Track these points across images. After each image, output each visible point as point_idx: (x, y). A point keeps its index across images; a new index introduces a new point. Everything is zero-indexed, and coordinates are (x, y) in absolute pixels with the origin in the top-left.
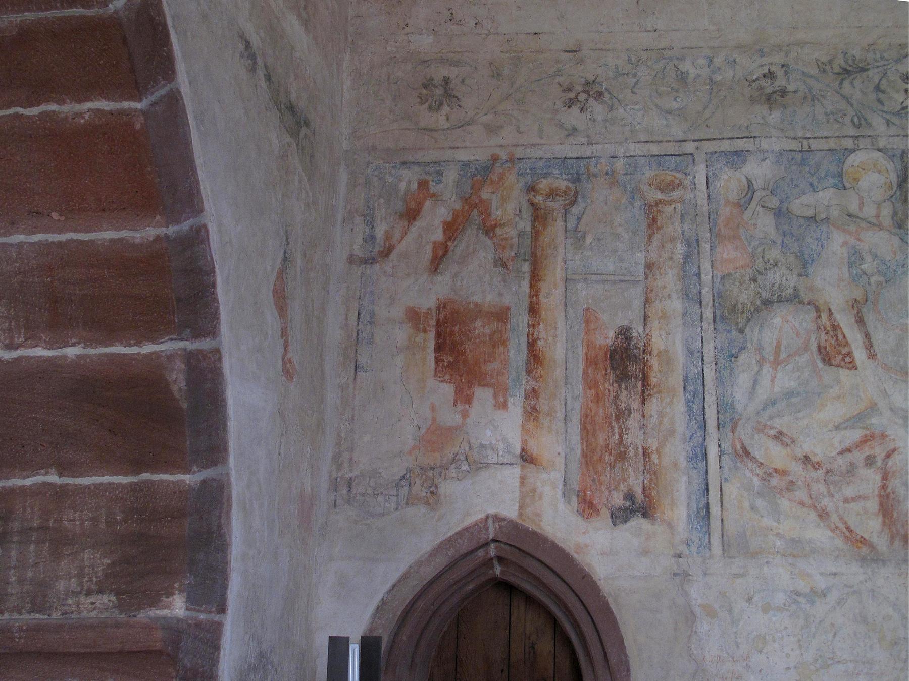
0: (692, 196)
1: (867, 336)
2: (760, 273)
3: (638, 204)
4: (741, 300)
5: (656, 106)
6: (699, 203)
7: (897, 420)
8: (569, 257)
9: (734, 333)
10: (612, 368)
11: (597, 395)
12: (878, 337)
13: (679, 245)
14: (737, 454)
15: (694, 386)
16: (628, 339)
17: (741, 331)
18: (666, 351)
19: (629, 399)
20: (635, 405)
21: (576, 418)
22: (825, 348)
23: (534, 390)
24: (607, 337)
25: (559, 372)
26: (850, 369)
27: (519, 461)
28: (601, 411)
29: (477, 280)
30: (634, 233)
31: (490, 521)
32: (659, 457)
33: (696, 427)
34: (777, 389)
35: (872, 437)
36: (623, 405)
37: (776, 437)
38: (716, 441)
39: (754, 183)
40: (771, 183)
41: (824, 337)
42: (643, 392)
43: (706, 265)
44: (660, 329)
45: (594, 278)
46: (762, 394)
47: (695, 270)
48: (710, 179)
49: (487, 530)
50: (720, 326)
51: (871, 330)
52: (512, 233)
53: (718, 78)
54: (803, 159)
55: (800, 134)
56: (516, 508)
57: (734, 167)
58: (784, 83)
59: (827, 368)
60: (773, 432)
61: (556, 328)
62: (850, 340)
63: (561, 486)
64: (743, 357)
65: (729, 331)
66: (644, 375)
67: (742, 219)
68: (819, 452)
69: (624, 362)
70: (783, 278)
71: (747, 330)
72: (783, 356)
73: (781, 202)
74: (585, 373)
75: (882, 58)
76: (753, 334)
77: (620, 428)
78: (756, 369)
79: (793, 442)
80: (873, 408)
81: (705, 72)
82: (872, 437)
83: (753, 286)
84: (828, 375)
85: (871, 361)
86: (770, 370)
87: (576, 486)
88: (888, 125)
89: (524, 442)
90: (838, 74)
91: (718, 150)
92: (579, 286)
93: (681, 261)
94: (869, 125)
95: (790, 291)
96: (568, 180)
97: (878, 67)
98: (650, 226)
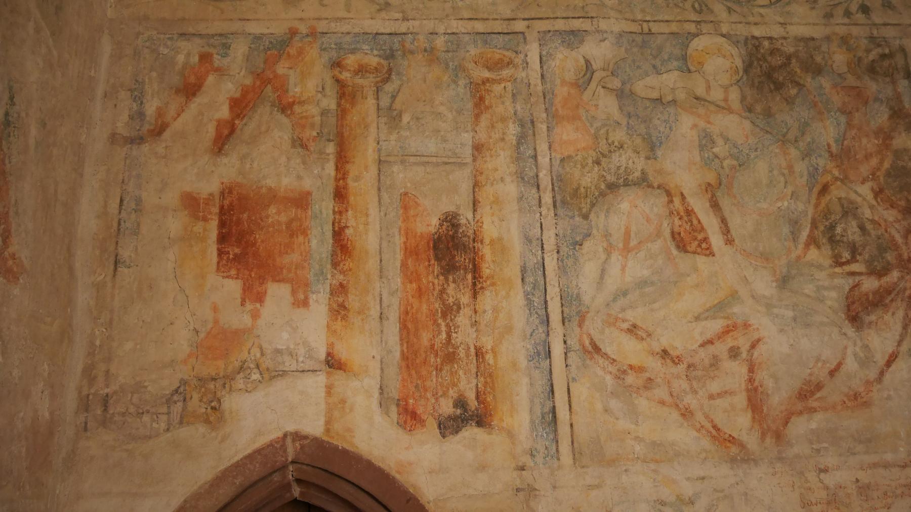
0: (524, 74)
1: (724, 221)
2: (604, 156)
3: (462, 82)
4: (583, 183)
6: (532, 82)
7: (760, 308)
8: (383, 137)
10: (437, 259)
11: (420, 289)
12: (735, 222)
13: (511, 126)
14: (585, 351)
16: (455, 226)
17: (586, 217)
18: (500, 239)
19: (458, 293)
20: (465, 299)
21: (393, 316)
22: (679, 234)
23: (341, 285)
24: (429, 224)
25: (372, 264)
27: (325, 367)
28: (424, 307)
29: (273, 162)
30: (459, 112)
31: (289, 440)
32: (495, 357)
33: (537, 322)
34: (628, 279)
36: (451, 300)
37: (629, 331)
39: (593, 63)
41: (677, 222)
42: (474, 284)
43: (542, 147)
44: (493, 215)
45: (412, 159)
46: (612, 283)
47: (530, 152)
48: (544, 59)
49: (285, 451)
50: (560, 211)
51: (727, 214)
54: (643, 41)
55: (639, 16)
57: (570, 46)
59: (682, 254)
60: (625, 326)
61: (367, 215)
62: (705, 226)
63: (376, 394)
64: (587, 245)
65: (572, 217)
66: (474, 265)
67: (581, 99)
68: (677, 344)
69: (451, 251)
70: (629, 160)
71: (592, 216)
72: (633, 243)
73: (623, 83)
74: (404, 265)
76: (598, 219)
77: (447, 325)
78: (603, 257)
82: (735, 326)
83: (596, 169)
84: (684, 262)
85: (728, 247)
86: (620, 257)
87: (395, 394)
89: (331, 345)
91: (552, 29)
92: (395, 169)
93: (514, 142)
95: (637, 174)
96: (380, 56)
98: (476, 105)
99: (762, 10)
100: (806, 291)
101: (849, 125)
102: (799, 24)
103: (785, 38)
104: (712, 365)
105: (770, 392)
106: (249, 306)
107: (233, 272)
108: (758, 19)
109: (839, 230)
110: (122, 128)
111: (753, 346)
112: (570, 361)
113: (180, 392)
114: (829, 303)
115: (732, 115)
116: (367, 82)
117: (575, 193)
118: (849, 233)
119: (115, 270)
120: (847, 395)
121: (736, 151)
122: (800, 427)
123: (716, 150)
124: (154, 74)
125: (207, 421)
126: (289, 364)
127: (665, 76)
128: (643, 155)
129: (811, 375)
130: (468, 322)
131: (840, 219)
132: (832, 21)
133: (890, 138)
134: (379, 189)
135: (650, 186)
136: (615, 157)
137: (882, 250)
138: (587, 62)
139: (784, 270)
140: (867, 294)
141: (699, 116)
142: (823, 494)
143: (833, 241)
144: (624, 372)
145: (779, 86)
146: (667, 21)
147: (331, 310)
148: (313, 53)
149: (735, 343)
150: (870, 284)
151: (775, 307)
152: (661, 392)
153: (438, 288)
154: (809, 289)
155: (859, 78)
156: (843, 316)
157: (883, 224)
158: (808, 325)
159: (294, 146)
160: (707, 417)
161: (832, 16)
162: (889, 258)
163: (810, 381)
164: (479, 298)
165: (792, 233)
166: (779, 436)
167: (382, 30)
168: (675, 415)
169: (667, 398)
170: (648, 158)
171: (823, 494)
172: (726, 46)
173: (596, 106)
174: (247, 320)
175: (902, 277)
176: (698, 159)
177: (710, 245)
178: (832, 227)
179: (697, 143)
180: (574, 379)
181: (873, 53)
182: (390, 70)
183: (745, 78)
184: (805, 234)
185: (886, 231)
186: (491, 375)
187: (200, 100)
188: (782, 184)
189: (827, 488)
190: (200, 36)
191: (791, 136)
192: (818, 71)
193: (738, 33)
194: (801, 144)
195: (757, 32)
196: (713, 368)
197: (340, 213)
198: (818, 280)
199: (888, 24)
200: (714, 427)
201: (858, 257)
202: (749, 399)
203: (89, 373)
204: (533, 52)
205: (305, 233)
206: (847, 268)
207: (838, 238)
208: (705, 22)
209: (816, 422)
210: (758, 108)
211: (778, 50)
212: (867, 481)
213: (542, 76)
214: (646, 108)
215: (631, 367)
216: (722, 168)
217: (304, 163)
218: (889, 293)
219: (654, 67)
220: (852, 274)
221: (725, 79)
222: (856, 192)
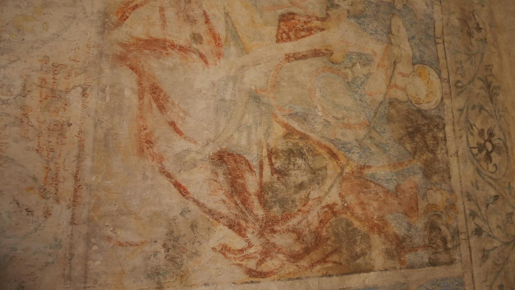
1: (304, 57)
7: (233, 70)
12: (304, 66)
22: (293, 19)
26: (277, 37)
35: (219, 45)
40: (411, 6)
41: (303, 19)
51: (310, 60)
55: (446, 38)
58: (475, 36)
59: (277, 17)
62: (299, 40)
73: (399, 11)
75: (500, 115)
80: (244, 50)
82: (219, 45)
84: (273, 16)
85: (284, 57)
88: (459, 110)
90: (487, 79)
94: (459, 94)
97: (495, 111)
99: (464, 138)
100: (247, 116)
101: (387, 192)
102: (459, 169)
103: (447, 153)
104: (188, 16)
105: (161, 60)
109: (300, 161)
111: (202, 56)
114: (236, 136)
115: (385, 86)
118: (297, 172)
120: (151, 133)
121: (359, 83)
122: (128, 80)
123: (358, 66)
127: (408, 43)
128: (350, 8)
129: (173, 104)
131: (309, 166)
133: (380, 232)
135: (328, 8)
139: (265, 100)
140: (242, 177)
141: (383, 59)
142: (62, 87)
143: (289, 154)
145: (411, 135)
146: (446, 58)
150: (252, 183)
151: (234, 85)
154: (249, 119)
155: (426, 213)
156: (224, 147)
157: (305, 209)
161: (469, 200)
162: (275, 209)
163: (168, 101)
165: (296, 114)
166: (122, 58)
170: (348, 11)
171: (62, 87)
172: (436, 99)
175: (258, 220)
176: (351, 49)
177: (285, 41)
178: (302, 155)
179: (362, 51)
181: (447, 231)
183: (414, 108)
184: (295, 125)
185: (299, 211)
188: (335, 115)
189: (67, 92)
191: (374, 134)
192: (427, 175)
193: (446, 112)
194: (369, 141)
196: (186, 18)
198: (256, 130)
199: (470, 251)
201: (276, 176)
202: (156, 40)
206: (266, 162)
207: (292, 160)
208: (450, 87)
209: (130, 96)
210: (393, 111)
212: (67, 134)
214: (384, 20)
216: (345, 68)
218: (244, 202)
219: (413, 38)
220: (261, 167)
222: (332, 186)
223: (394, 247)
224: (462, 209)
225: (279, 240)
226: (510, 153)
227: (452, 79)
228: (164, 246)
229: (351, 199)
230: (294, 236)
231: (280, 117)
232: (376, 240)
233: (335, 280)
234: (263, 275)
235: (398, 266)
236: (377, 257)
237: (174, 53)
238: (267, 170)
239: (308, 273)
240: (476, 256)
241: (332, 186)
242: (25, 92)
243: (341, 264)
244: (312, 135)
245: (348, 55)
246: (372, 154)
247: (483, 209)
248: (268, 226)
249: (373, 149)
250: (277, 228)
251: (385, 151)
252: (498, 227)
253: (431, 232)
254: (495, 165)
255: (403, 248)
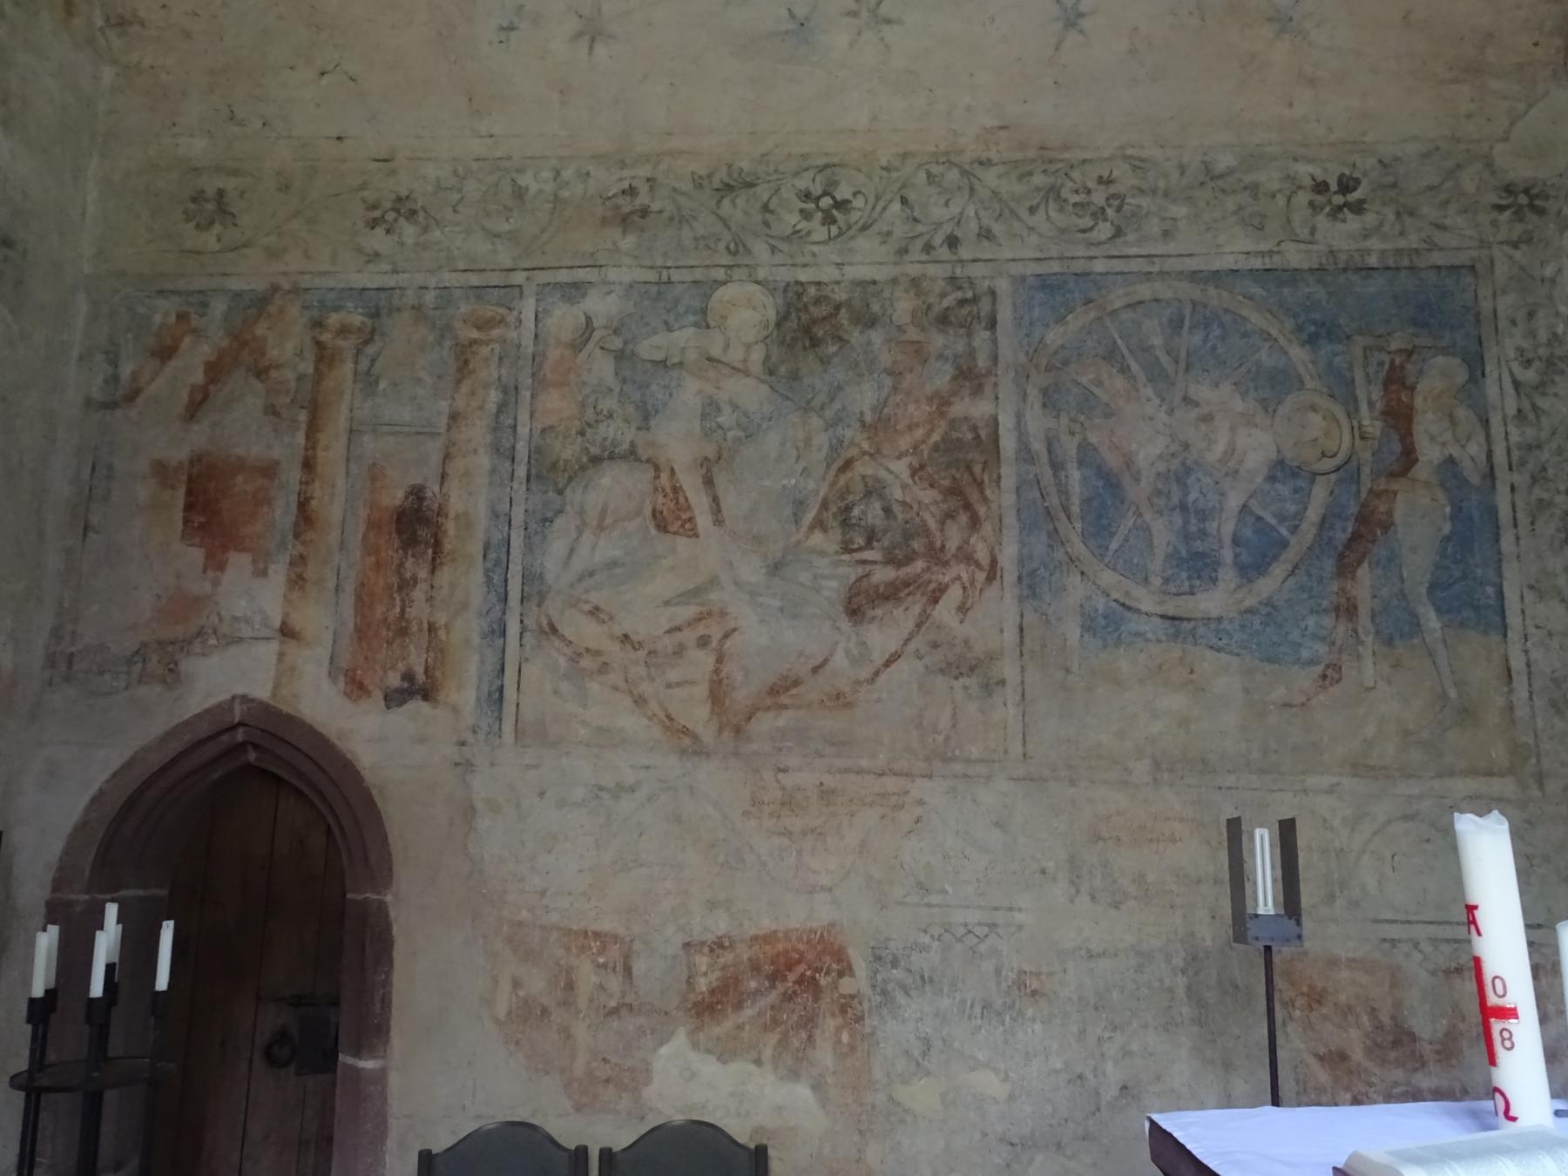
0: (515, 335)
1: (715, 499)
2: (589, 425)
3: (447, 344)
4: (564, 456)
5: (483, 228)
9: (551, 494)
10: (399, 532)
11: (378, 562)
12: (729, 500)
15: (497, 556)
16: (421, 499)
17: (560, 492)
20: (423, 574)
21: (349, 588)
24: (395, 497)
25: (334, 536)
32: (448, 632)
35: (710, 614)
36: (408, 575)
37: (591, 613)
38: (518, 618)
41: (661, 500)
42: (434, 559)
45: (385, 429)
46: (578, 565)
47: (510, 422)
50: (533, 486)
52: (290, 375)
53: (565, 194)
54: (659, 293)
55: (659, 262)
56: (269, 687)
57: (571, 301)
60: (587, 607)
61: (334, 486)
63: (326, 664)
64: (559, 522)
65: (546, 492)
69: (415, 525)
70: (618, 431)
71: (568, 492)
72: (608, 521)
73: (626, 343)
74: (365, 537)
75: (776, 171)
76: (574, 495)
77: (403, 601)
78: (574, 534)
79: (611, 618)
80: (714, 582)
81: (549, 187)
82: (710, 614)
87: (344, 661)
89: (287, 615)
92: (366, 438)
94: (749, 252)
95: (626, 446)
98: (460, 370)
99: (815, 248)
101: (895, 389)
102: (862, 264)
103: (838, 283)
106: (210, 574)
107: (197, 540)
108: (808, 259)
109: (856, 512)
110: (97, 394)
111: (726, 636)
112: (525, 641)
113: (141, 653)
114: (826, 593)
116: (347, 344)
117: (554, 465)
119: (85, 535)
122: (765, 723)
124: (130, 336)
125: (164, 682)
126: (246, 631)
127: (677, 333)
128: (634, 425)
130: (423, 597)
132: (906, 258)
134: (348, 460)
135: (638, 460)
136: (602, 427)
137: (908, 536)
138: (588, 318)
140: (877, 587)
144: (580, 655)
145: (815, 343)
147: (289, 580)
148: (294, 310)
149: (706, 632)
150: (883, 575)
152: (615, 678)
153: (396, 562)
154: (805, 577)
155: (923, 330)
157: (916, 507)
158: (795, 617)
159: (266, 413)
160: (661, 705)
161: (906, 251)
164: (438, 573)
165: (795, 514)
167: (369, 286)
168: (627, 702)
169: (623, 686)
170: (639, 429)
171: (779, 794)
173: (589, 370)
174: (208, 587)
175: (929, 568)
178: (848, 509)
180: (527, 660)
182: (373, 332)
184: (810, 515)
186: (442, 651)
187: (175, 363)
188: (793, 460)
190: (179, 293)
191: (817, 402)
192: (872, 322)
195: (803, 276)
197: (307, 483)
200: (668, 716)
202: (711, 691)
203: (56, 633)
204: (528, 307)
205: (269, 502)
208: (739, 266)
209: (783, 720)
210: (783, 370)
211: (826, 297)
213: (536, 336)
215: (588, 650)
217: (275, 431)
218: (907, 585)
219: (666, 323)
220: (864, 562)
221: (750, 336)
222: (888, 469)
223: (967, 384)
224: (919, 266)
225: (952, 545)
226: (835, 160)
227: (726, 260)
228: (956, 678)
229: (904, 443)
230: (949, 522)
231: (800, 536)
232: (958, 409)
233: (1005, 470)
234: (994, 562)
235: (993, 379)
236: (980, 409)
237: (725, 670)
238: (868, 555)
239: (994, 506)
240: (986, 250)
241: (888, 469)
242: (787, 833)
243: (985, 463)
244: (822, 494)
245: (707, 434)
246: (844, 408)
247: (920, 228)
248: (936, 555)
249: (837, 405)
250: (938, 544)
251: (840, 388)
252: (947, 204)
253: (950, 323)
254: (855, 194)
255: (970, 370)
